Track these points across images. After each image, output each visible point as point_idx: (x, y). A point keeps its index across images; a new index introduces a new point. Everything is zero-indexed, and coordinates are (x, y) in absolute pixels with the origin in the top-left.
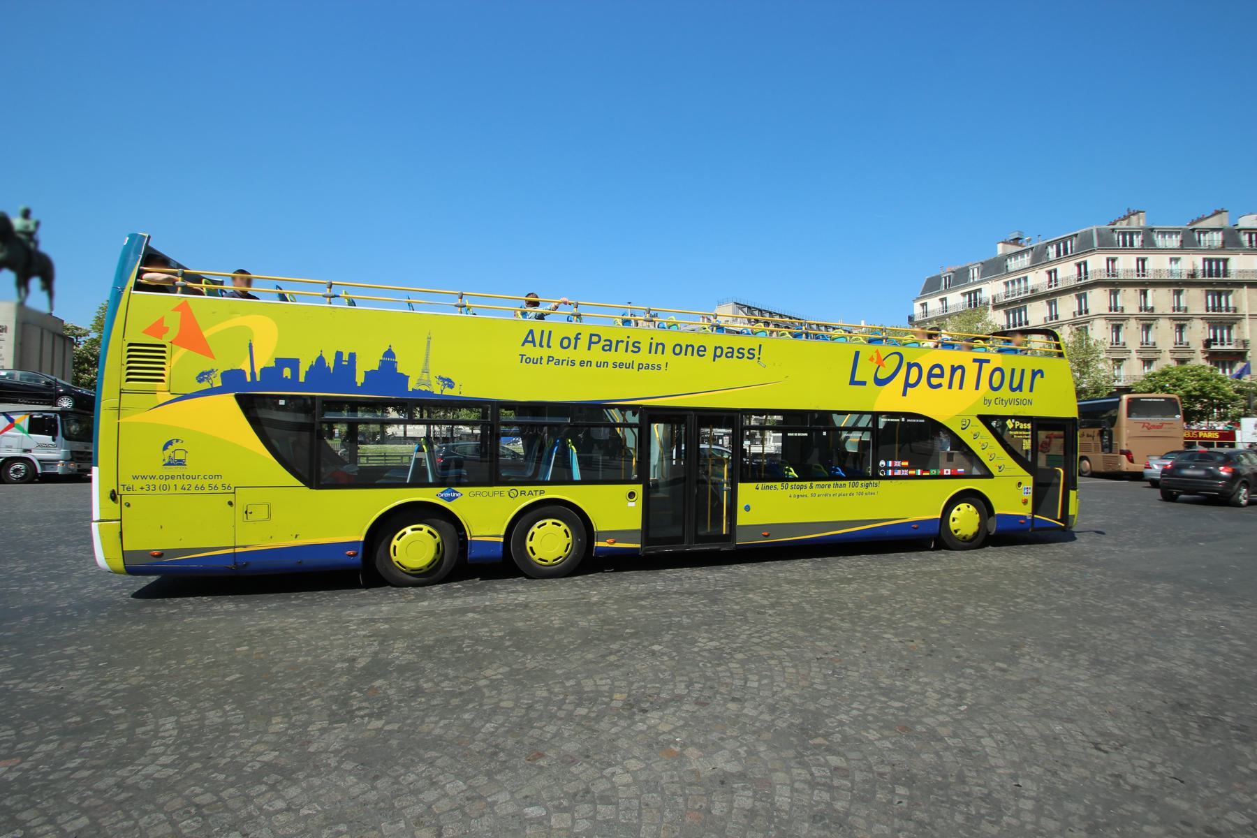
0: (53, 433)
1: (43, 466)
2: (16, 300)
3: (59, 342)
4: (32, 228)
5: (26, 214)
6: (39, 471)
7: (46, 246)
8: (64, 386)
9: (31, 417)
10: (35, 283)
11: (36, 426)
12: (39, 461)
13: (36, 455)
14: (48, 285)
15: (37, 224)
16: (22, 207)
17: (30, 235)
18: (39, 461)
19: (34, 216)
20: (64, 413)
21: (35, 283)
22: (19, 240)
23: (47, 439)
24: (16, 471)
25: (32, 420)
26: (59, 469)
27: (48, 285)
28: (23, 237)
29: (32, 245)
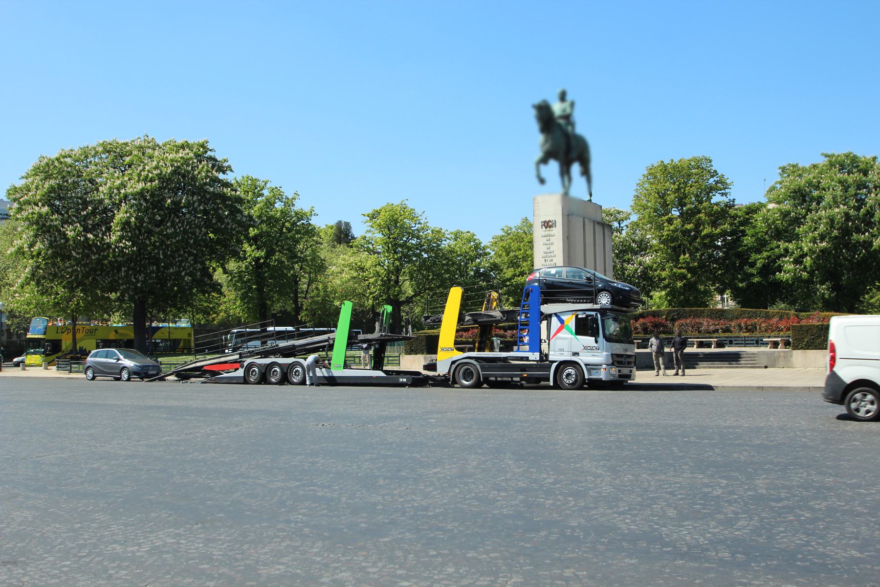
0: (594, 334)
1: (589, 370)
2: (560, 190)
3: (599, 229)
4: (568, 111)
5: (563, 97)
6: (586, 377)
7: (582, 128)
8: (602, 280)
9: (577, 316)
10: (576, 168)
11: (584, 327)
12: (586, 365)
13: (584, 359)
14: (586, 172)
15: (572, 105)
16: (559, 90)
17: (567, 117)
18: (586, 365)
19: (569, 98)
20: (603, 311)
21: (576, 168)
22: (559, 126)
23: (589, 340)
24: (568, 375)
25: (578, 321)
26: (602, 375)
27: (586, 172)
28: (562, 122)
29: (569, 128)
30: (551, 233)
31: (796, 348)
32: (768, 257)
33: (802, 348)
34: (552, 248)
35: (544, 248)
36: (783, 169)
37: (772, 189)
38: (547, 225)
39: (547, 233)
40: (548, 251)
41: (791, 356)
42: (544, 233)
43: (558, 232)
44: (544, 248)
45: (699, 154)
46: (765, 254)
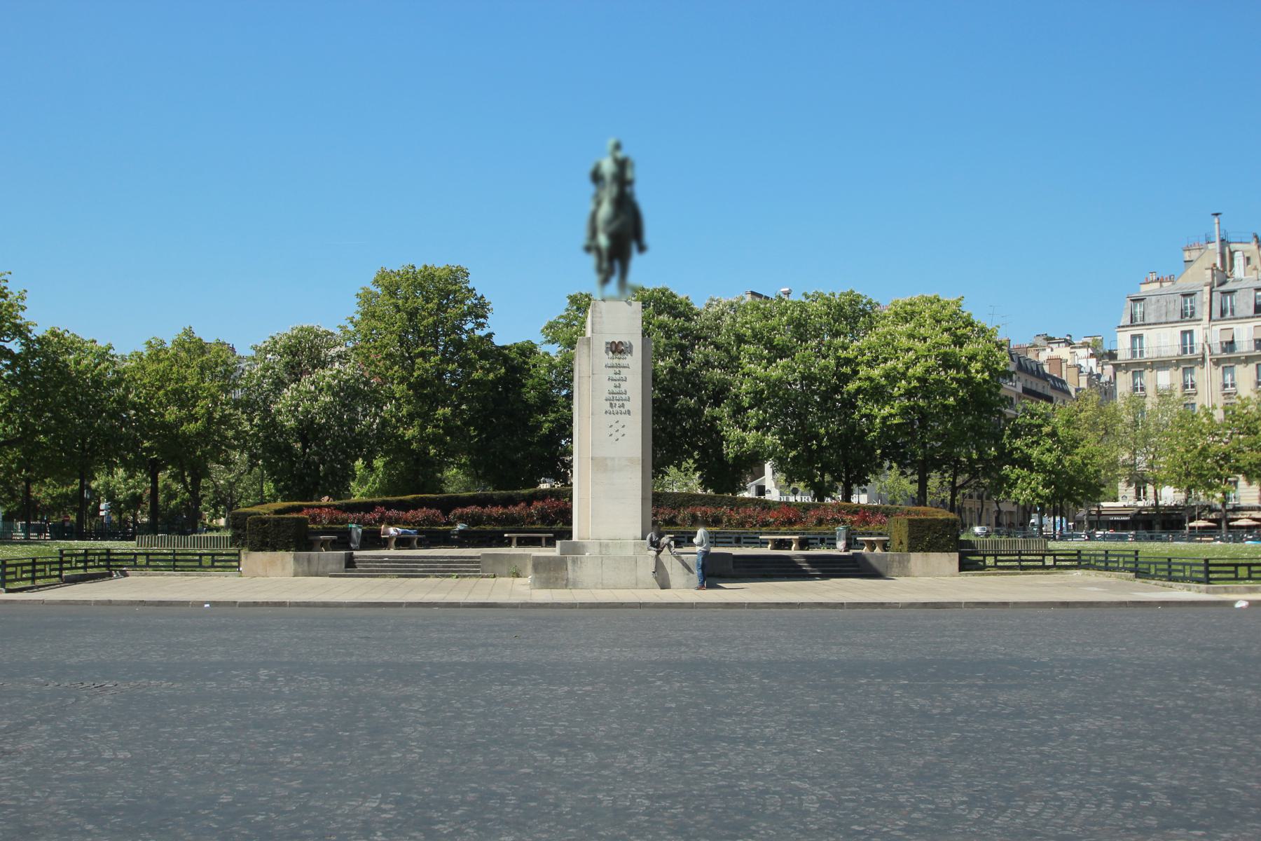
30: (622, 362)
31: (912, 548)
32: (557, 420)
33: (922, 550)
34: (624, 386)
35: (610, 386)
36: (574, 300)
37: (551, 326)
38: (617, 349)
39: (616, 361)
40: (617, 390)
41: (908, 561)
42: (610, 362)
43: (634, 362)
44: (610, 386)
45: (454, 263)
46: (552, 416)
